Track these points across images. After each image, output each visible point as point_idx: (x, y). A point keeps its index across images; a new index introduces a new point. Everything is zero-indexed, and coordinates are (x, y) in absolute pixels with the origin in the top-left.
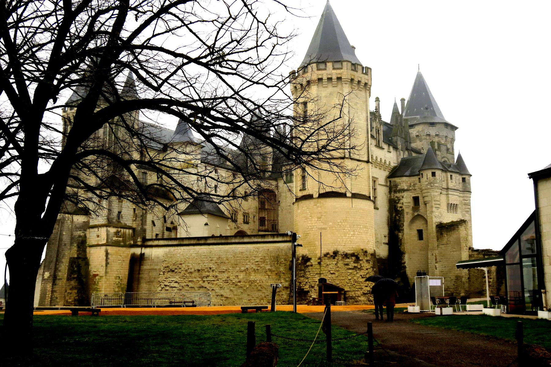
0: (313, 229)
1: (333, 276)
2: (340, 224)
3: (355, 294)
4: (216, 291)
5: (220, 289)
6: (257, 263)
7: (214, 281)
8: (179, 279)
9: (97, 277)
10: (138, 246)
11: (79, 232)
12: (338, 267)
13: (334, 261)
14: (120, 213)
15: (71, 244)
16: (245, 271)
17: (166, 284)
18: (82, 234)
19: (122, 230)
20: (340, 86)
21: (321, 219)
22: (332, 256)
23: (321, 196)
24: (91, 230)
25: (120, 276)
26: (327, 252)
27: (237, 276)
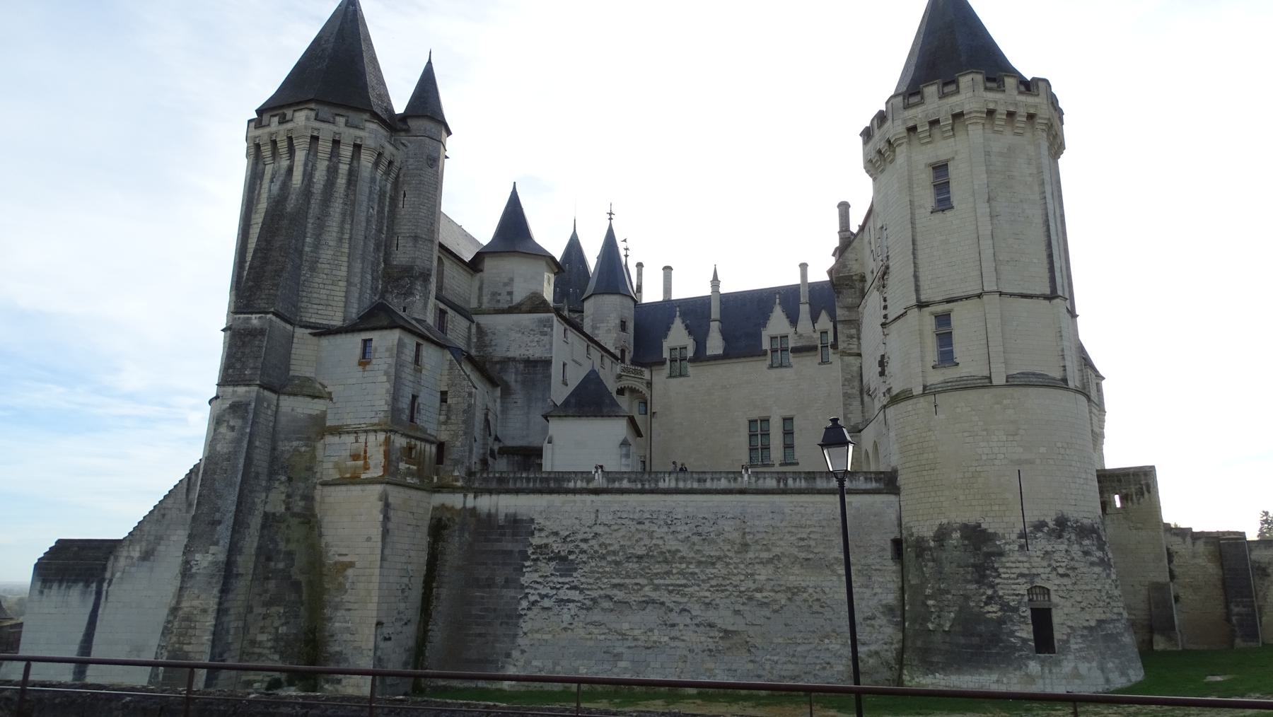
0: (997, 462)
1: (1065, 581)
2: (1062, 451)
3: (1115, 627)
4: (694, 613)
5: (703, 607)
6: (802, 543)
7: (685, 586)
8: (583, 580)
9: (350, 572)
10: (453, 490)
11: (295, 444)
12: (1072, 559)
13: (1062, 543)
14: (414, 397)
15: (272, 475)
16: (770, 561)
17: (544, 592)
18: (303, 449)
19: (418, 443)
20: (1028, 135)
21: (1017, 438)
22: (1053, 530)
23: (1014, 381)
24: (330, 439)
25: (410, 567)
26: (1042, 519)
27: (752, 575)
